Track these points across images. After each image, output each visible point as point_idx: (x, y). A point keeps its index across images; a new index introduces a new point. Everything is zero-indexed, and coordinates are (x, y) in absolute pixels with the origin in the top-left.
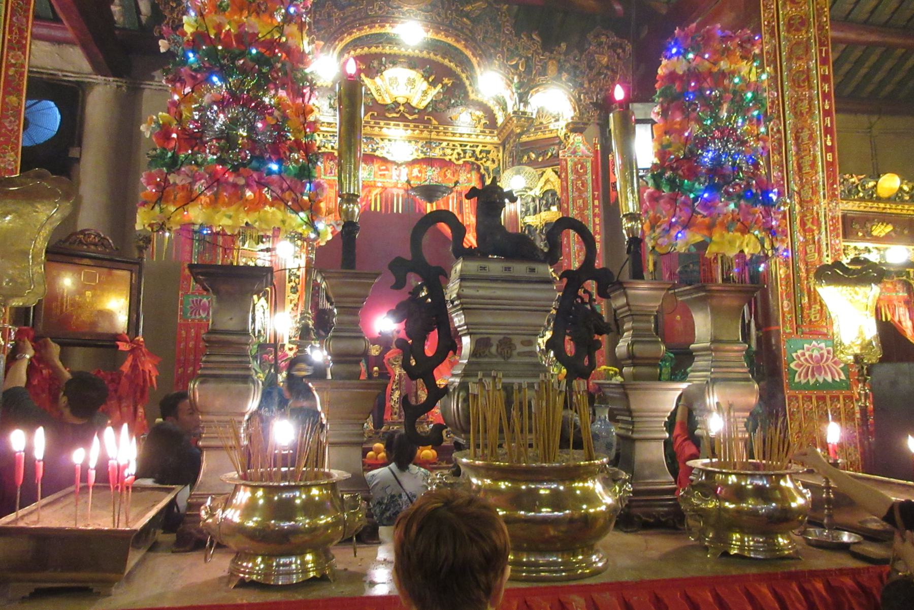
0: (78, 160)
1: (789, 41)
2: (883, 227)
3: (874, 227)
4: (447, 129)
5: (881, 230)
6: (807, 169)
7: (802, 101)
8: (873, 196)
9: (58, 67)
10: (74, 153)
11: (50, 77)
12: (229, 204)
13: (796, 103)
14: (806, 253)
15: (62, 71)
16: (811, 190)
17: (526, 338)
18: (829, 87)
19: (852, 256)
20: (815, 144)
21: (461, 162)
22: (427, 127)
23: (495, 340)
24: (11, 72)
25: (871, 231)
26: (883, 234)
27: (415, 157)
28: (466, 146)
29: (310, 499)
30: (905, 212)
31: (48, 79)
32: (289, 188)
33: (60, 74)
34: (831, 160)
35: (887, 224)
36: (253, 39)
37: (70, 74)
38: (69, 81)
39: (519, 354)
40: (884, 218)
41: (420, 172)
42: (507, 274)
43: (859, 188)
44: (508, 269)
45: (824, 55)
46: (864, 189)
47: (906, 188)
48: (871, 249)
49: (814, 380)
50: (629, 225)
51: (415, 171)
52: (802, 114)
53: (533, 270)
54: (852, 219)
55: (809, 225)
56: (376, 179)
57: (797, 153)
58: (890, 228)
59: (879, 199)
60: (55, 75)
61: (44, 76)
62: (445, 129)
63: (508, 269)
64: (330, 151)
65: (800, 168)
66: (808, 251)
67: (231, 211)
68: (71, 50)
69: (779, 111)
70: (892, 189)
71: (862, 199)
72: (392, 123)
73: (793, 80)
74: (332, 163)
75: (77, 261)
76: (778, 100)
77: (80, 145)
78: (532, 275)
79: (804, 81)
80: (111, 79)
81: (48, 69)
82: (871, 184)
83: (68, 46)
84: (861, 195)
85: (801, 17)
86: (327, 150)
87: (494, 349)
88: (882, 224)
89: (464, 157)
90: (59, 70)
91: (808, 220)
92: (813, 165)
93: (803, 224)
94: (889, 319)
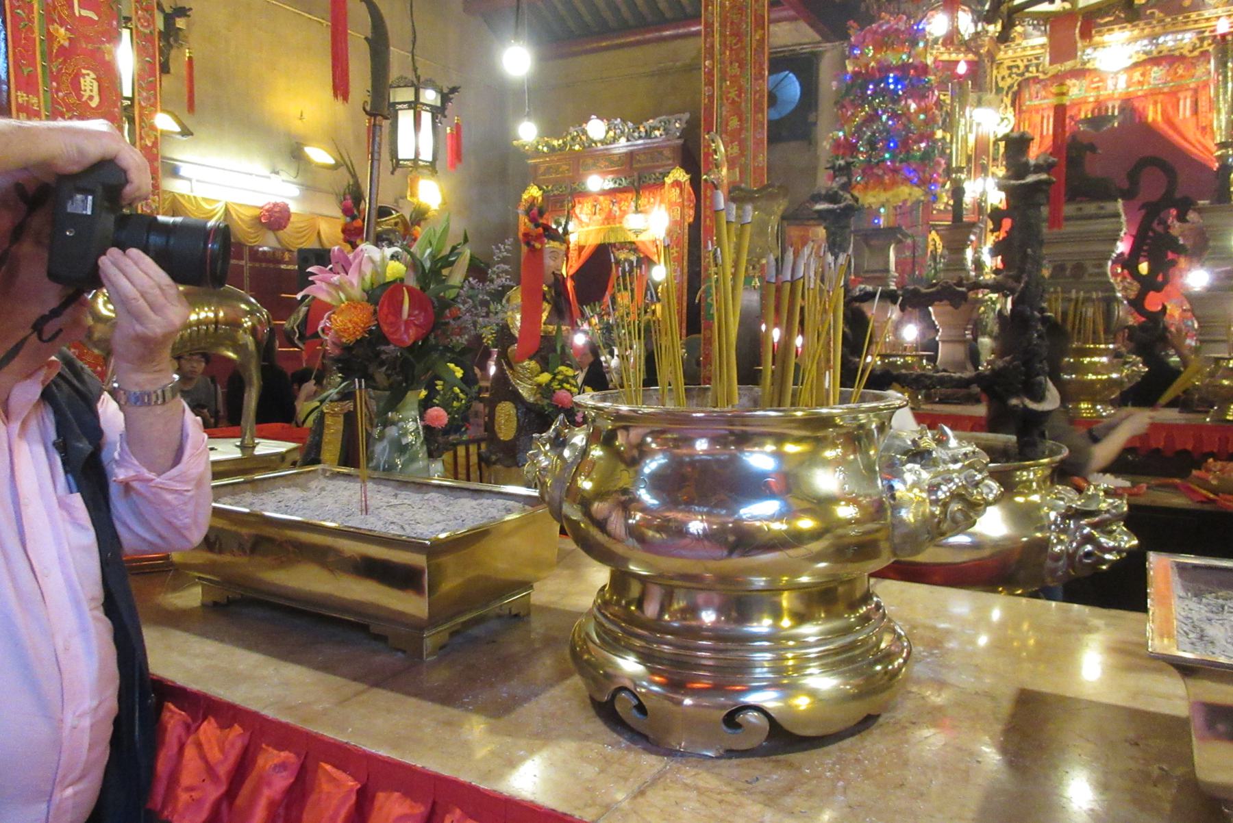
0: (815, 124)
4: (1176, 19)
9: (795, 41)
10: (811, 118)
12: (873, 188)
15: (800, 44)
17: (1097, 262)
21: (1196, 53)
22: (1150, 23)
23: (1069, 265)
24: (757, 96)
27: (1134, 60)
28: (1204, 32)
29: (905, 362)
32: (914, 170)
33: (798, 48)
36: (890, 68)
39: (1091, 275)
41: (1143, 75)
42: (1079, 213)
44: (1080, 209)
50: (1219, 153)
51: (1137, 75)
53: (1102, 208)
56: (1087, 95)
61: (786, 54)
62: (1173, 19)
63: (1080, 209)
64: (1035, 74)
67: (874, 193)
72: (1105, 29)
74: (1038, 86)
75: (806, 223)
77: (816, 110)
78: (1103, 212)
80: (837, 43)
86: (1031, 75)
87: (1068, 272)
89: (1201, 47)
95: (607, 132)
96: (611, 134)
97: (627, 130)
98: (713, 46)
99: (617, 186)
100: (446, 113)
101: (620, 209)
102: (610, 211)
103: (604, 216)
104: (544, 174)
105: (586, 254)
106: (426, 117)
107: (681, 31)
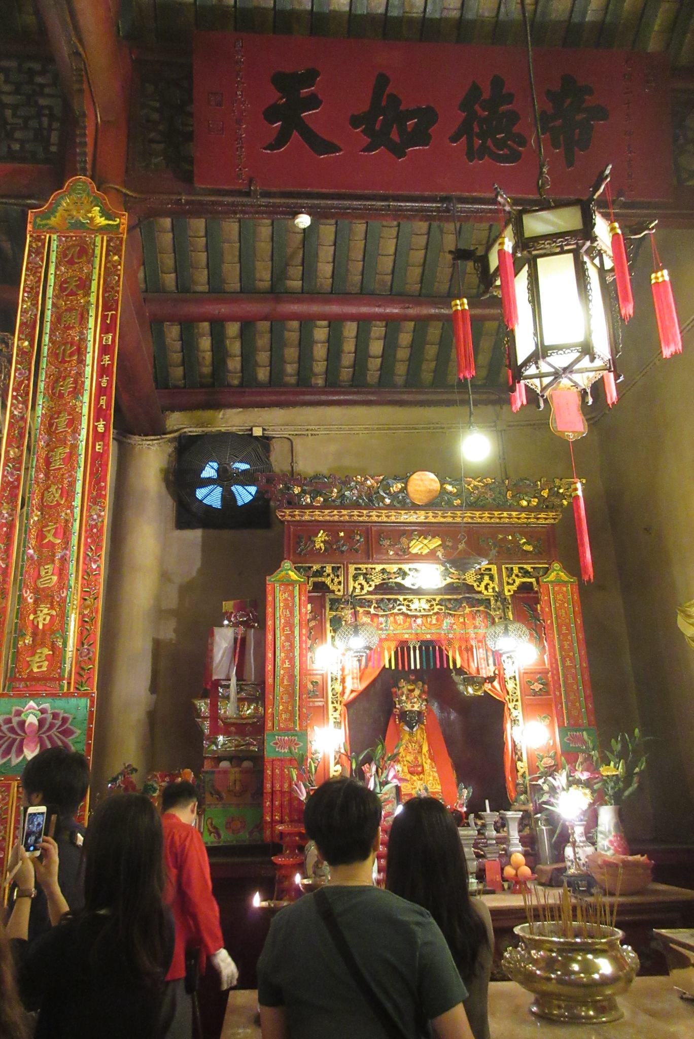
1: (58, 308)
2: (426, 542)
3: (412, 543)
5: (418, 546)
6: (57, 464)
7: (64, 379)
8: (403, 502)
13: (57, 381)
14: (39, 576)
16: (60, 492)
18: (112, 359)
19: (378, 581)
20: (76, 431)
25: (409, 548)
26: (425, 551)
30: (458, 520)
34: (101, 451)
35: (433, 537)
40: (427, 530)
43: (382, 493)
45: (108, 322)
46: (389, 494)
47: (449, 488)
48: (407, 570)
49: (21, 757)
52: (61, 396)
54: (379, 534)
55: (50, 537)
57: (48, 445)
58: (437, 542)
59: (415, 507)
65: (48, 462)
66: (43, 573)
69: (27, 394)
70: (430, 491)
71: (389, 507)
73: (57, 355)
76: (29, 380)
79: (71, 355)
82: (397, 487)
84: (388, 501)
85: (80, 279)
88: (425, 538)
91: (49, 531)
92: (71, 458)
93: (41, 536)
94: (458, 666)
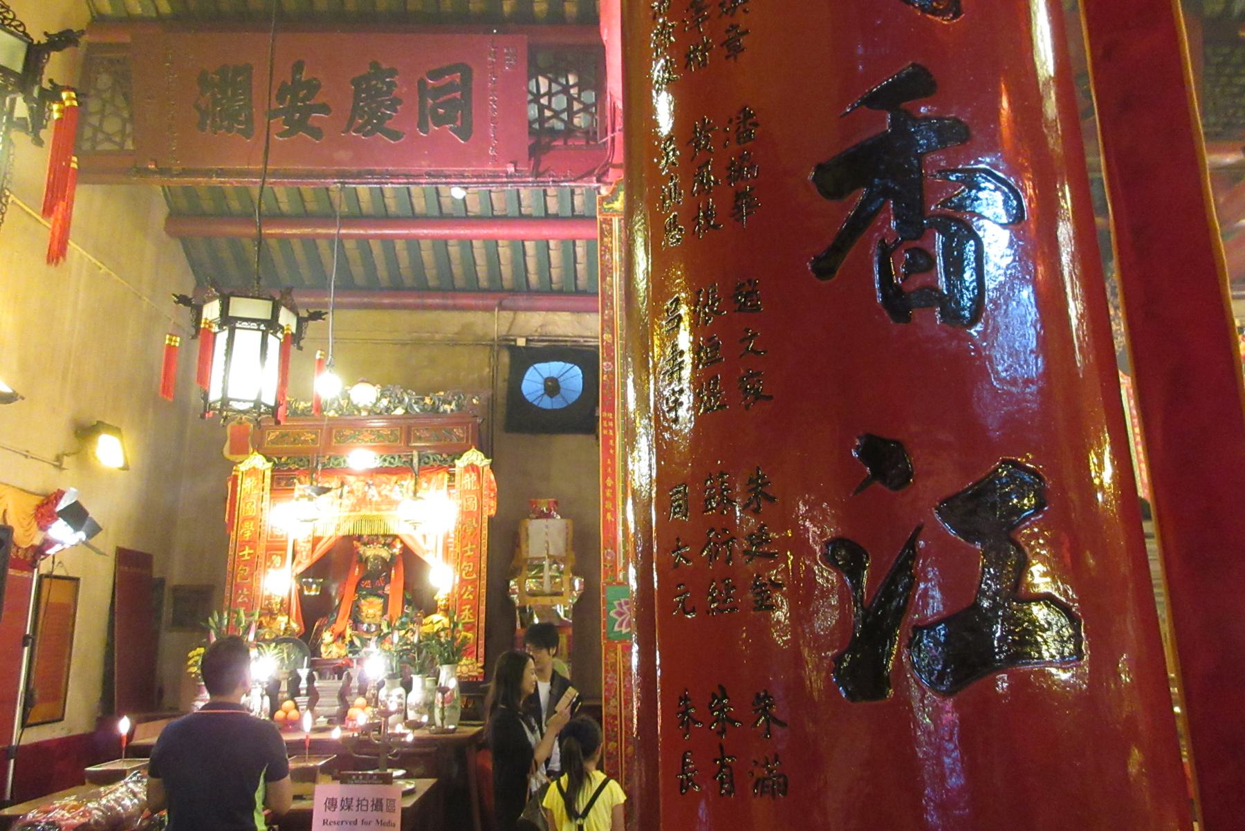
9: (576, 333)
11: (574, 344)
15: (583, 337)
31: (573, 346)
33: (582, 340)
37: (589, 340)
38: (588, 346)
60: (575, 341)
61: (569, 344)
68: (588, 316)
81: (568, 336)
83: (585, 314)
90: (580, 337)
95: (378, 400)
96: (385, 402)
97: (407, 400)
98: (612, 319)
99: (386, 464)
100: (302, 343)
101: (379, 493)
102: (365, 494)
103: (353, 500)
104: (272, 442)
105: (321, 548)
106: (274, 343)
107: (450, 302)
